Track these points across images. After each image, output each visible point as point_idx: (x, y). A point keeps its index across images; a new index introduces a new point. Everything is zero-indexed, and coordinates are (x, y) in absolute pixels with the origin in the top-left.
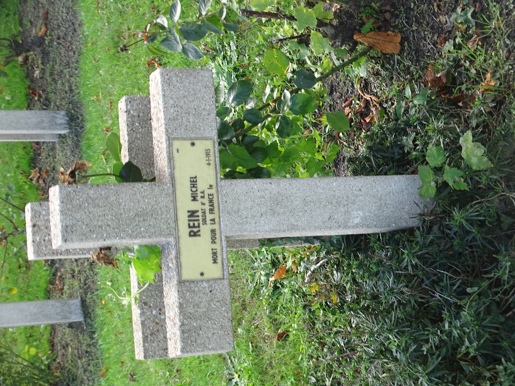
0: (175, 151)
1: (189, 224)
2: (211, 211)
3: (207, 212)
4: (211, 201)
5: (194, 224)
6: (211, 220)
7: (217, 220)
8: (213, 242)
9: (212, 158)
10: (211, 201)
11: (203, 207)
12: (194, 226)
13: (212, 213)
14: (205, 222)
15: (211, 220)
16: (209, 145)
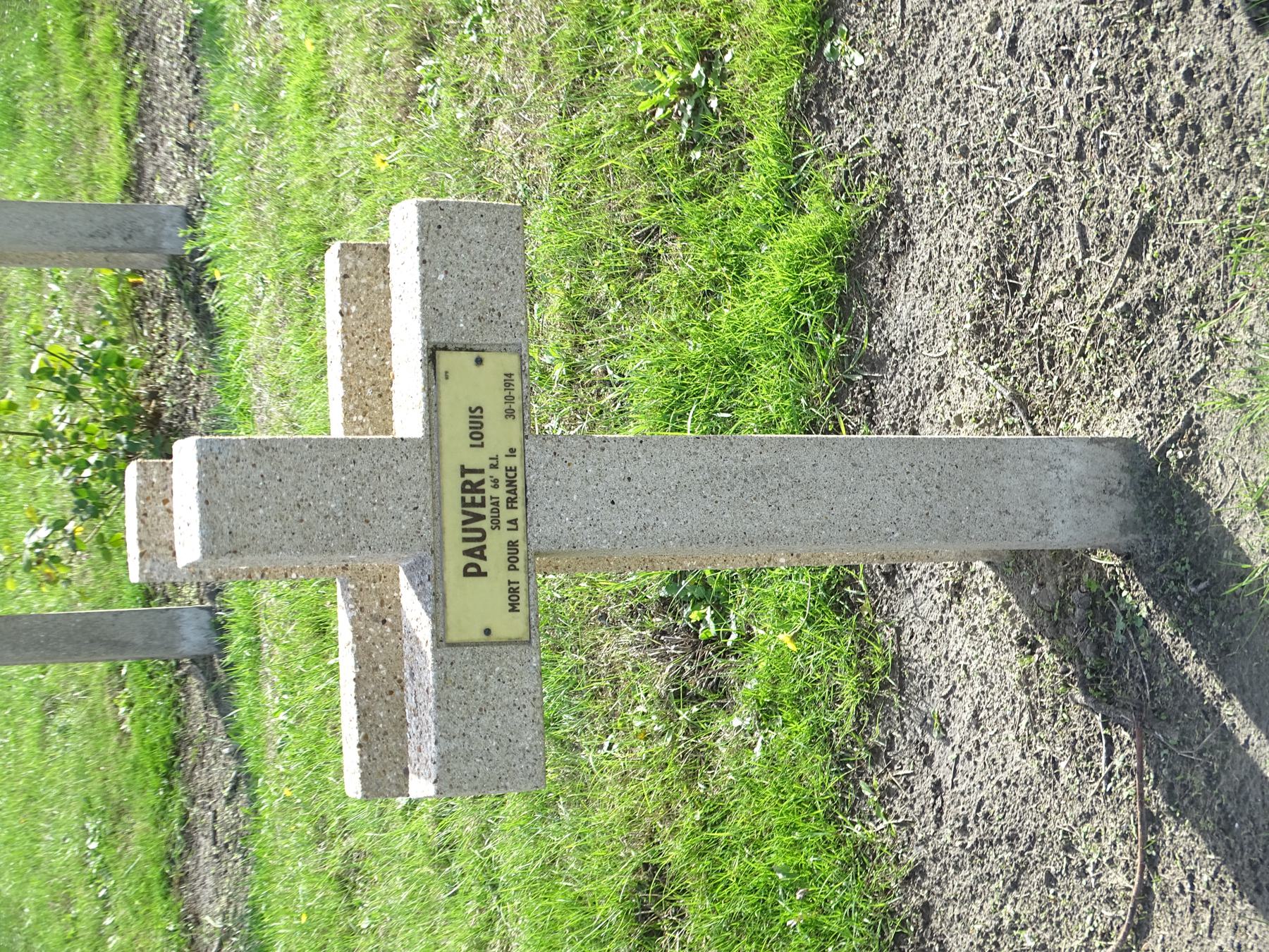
0: (441, 375)
1: (463, 499)
2: (511, 503)
3: (503, 503)
4: (511, 482)
5: (473, 498)
6: (510, 522)
7: (521, 523)
8: (512, 567)
9: (517, 392)
10: (511, 482)
11: (495, 493)
12: (473, 504)
13: (512, 508)
14: (496, 525)
15: (510, 522)
16: (510, 362)
